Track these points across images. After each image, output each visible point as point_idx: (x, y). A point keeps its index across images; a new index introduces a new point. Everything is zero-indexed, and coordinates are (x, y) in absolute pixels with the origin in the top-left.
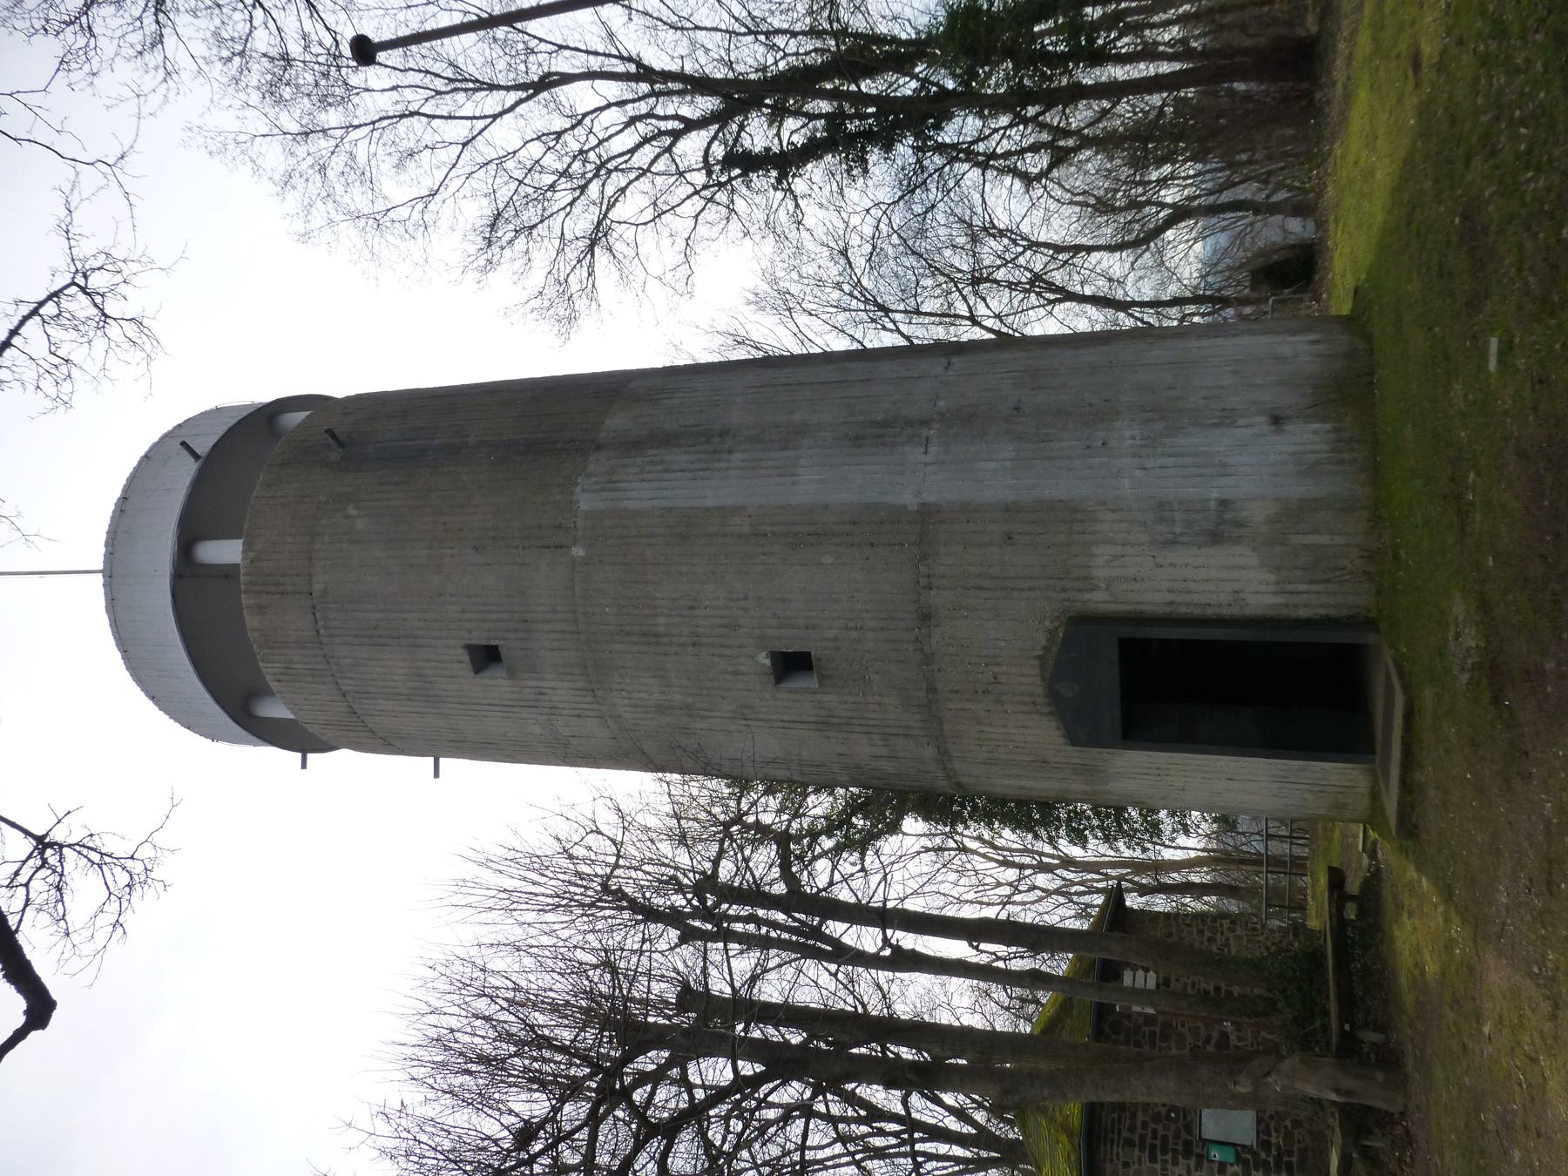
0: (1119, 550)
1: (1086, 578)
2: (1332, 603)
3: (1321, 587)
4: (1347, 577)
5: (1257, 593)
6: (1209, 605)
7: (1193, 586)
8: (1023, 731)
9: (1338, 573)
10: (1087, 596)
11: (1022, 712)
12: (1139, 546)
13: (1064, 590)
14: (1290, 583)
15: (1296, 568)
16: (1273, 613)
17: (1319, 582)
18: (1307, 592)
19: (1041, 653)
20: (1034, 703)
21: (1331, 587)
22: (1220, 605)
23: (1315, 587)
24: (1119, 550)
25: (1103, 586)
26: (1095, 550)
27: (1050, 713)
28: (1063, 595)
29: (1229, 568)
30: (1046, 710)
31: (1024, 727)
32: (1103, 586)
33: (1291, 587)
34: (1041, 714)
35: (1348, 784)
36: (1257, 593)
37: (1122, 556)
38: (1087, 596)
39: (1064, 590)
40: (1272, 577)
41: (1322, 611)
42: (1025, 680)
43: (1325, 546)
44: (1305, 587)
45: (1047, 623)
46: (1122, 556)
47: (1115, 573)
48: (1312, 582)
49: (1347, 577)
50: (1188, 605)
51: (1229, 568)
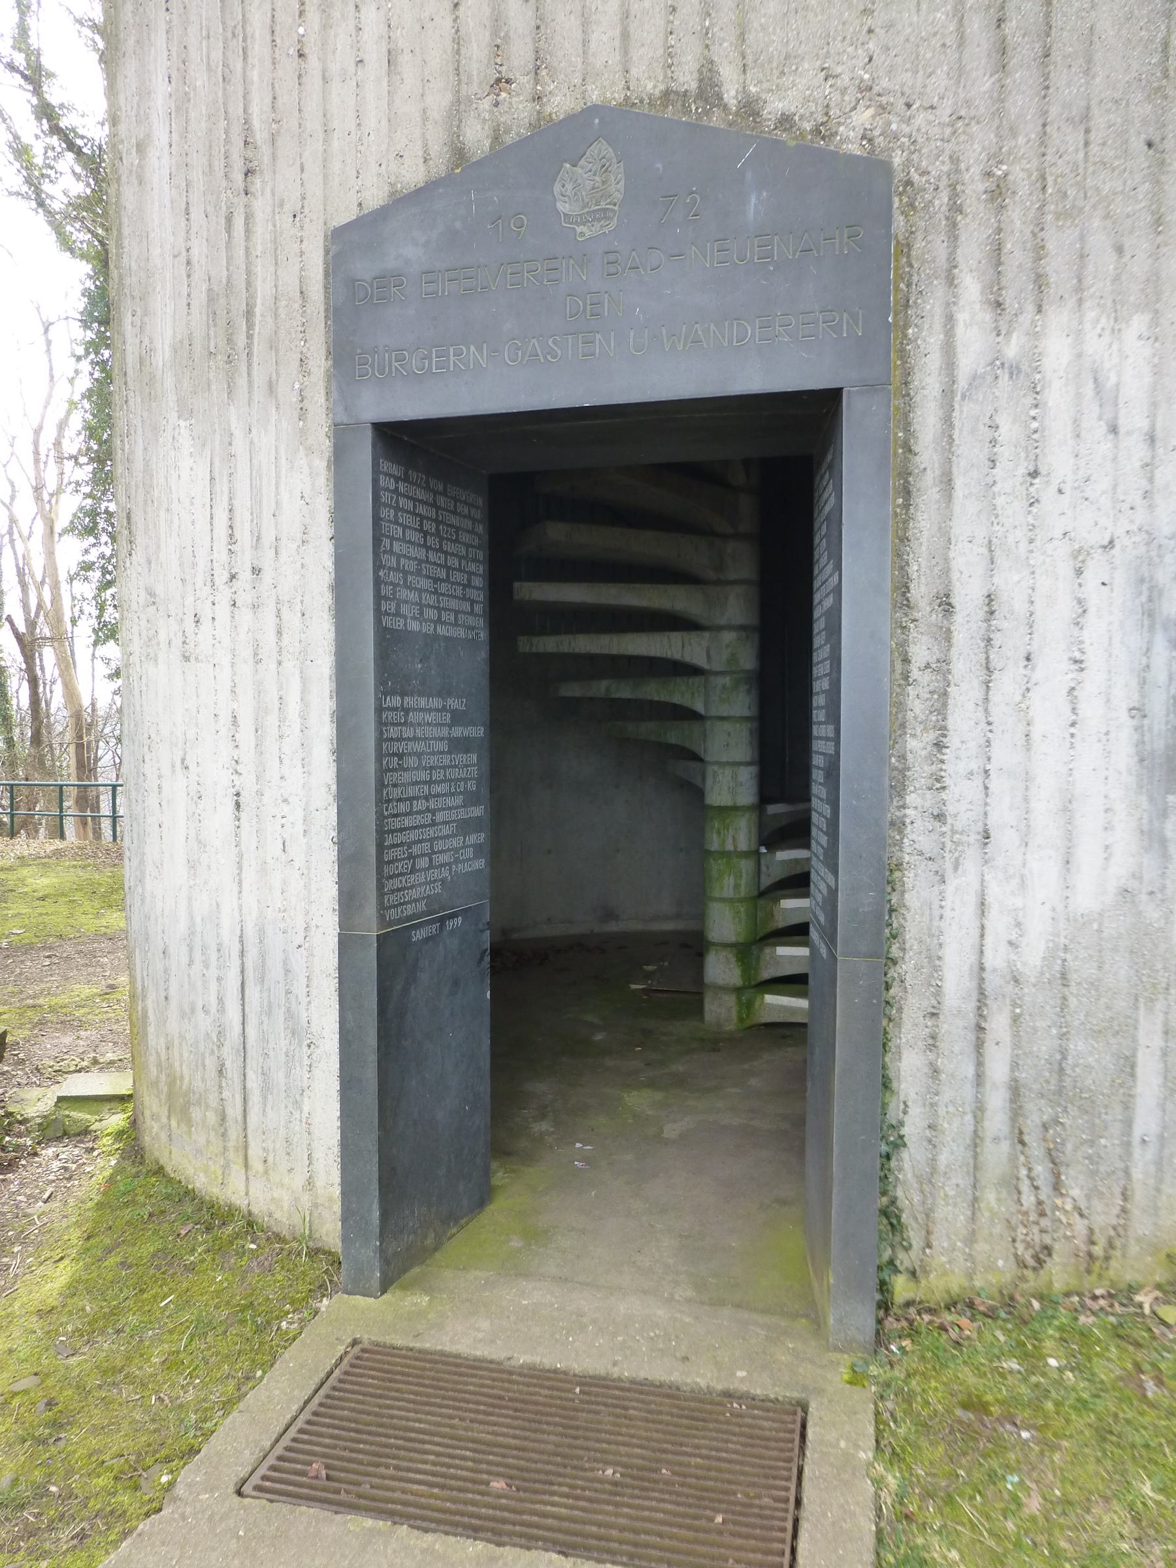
0: (1134, 420)
1: (1040, 281)
2: (943, 1159)
3: (997, 1121)
4: (1028, 1200)
5: (982, 907)
6: (939, 746)
7: (1007, 685)
8: (374, 55)
9: (1041, 1170)
10: (971, 287)
11: (458, 40)
12: (1146, 495)
13: (998, 193)
14: (1016, 1019)
15: (1062, 1036)
16: (909, 966)
17: (1016, 1112)
18: (979, 1079)
19: (730, 95)
20: (501, 82)
21: (997, 1154)
22: (938, 783)
23: (997, 1101)
24: (1134, 420)
25: (1013, 349)
26: (1139, 323)
27: (459, 153)
28: (974, 187)
29: (1067, 808)
30: (476, 137)
31: (391, 60)
32: (1013, 349)
33: (999, 1024)
34: (458, 108)
35: (255, 1151)
36: (982, 907)
37: (1114, 430)
38: (971, 287)
39: (998, 193)
40: (1032, 958)
41: (913, 1128)
42: (604, 37)
43: (1128, 1123)
44: (998, 1068)
45: (863, 117)
46: (1114, 430)
47: (1057, 397)
48: (1015, 1090)
49: (1028, 1200)
50: (941, 668)
51: (1067, 808)
